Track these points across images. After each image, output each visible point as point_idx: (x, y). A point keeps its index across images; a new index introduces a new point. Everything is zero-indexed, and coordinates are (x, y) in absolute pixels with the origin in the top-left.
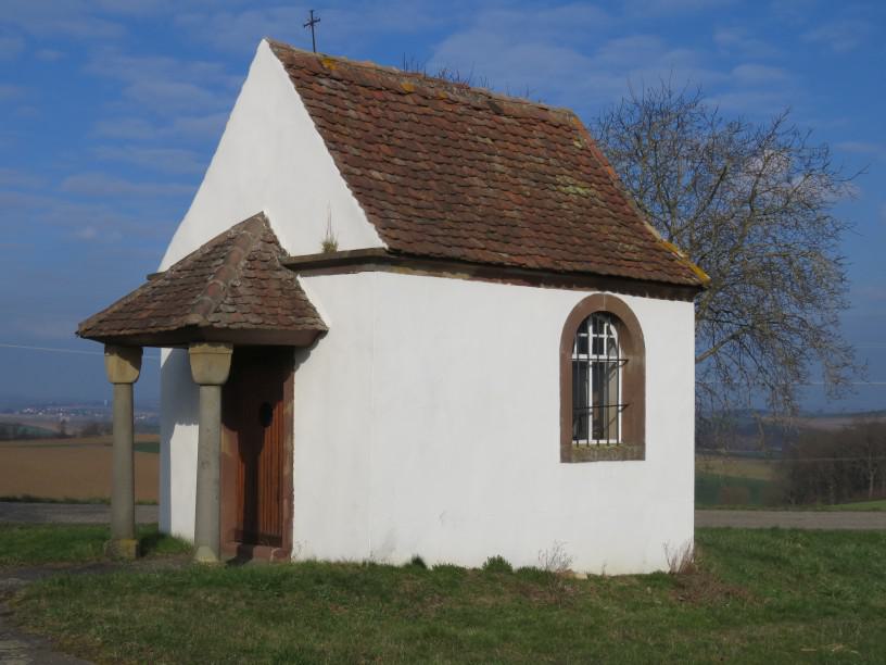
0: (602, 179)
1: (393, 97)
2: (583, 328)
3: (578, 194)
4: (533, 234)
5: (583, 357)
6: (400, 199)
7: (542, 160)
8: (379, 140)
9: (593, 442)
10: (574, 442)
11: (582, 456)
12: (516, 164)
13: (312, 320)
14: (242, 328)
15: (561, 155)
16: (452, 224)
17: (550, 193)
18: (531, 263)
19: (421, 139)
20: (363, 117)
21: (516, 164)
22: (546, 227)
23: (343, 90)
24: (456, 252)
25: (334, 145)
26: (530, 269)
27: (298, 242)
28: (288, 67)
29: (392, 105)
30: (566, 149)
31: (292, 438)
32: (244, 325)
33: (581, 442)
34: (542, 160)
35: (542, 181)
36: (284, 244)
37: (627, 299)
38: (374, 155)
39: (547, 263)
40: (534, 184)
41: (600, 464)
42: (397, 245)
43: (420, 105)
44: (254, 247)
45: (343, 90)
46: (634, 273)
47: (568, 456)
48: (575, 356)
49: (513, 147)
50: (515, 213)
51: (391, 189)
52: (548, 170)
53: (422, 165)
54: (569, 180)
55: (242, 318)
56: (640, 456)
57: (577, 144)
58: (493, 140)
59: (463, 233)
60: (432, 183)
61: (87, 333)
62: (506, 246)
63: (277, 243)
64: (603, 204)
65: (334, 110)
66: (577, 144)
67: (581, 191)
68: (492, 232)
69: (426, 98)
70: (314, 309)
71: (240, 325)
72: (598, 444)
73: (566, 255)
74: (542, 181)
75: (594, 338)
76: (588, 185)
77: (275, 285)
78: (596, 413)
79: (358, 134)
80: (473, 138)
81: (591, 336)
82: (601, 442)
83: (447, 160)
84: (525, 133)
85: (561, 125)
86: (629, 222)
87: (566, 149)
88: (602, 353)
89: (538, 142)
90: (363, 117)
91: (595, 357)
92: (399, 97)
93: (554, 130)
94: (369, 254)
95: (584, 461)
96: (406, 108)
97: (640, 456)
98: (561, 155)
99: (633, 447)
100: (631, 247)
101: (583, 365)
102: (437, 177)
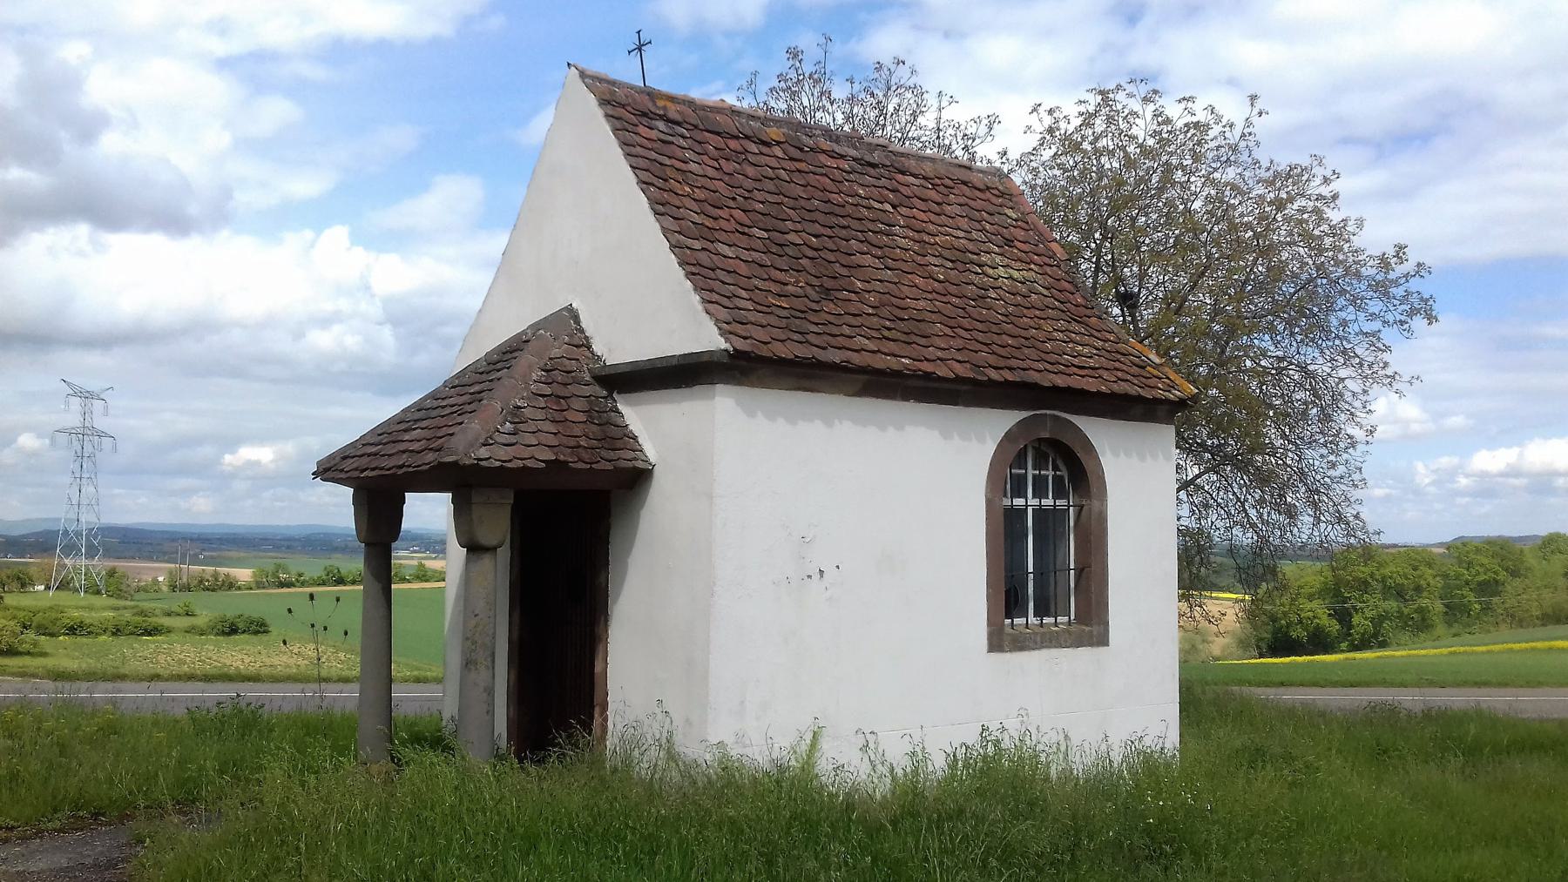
0: (1047, 260)
1: (753, 148)
2: (1020, 460)
3: (1011, 277)
4: (948, 331)
5: (1019, 502)
6: (756, 282)
7: (961, 234)
8: (731, 203)
9: (1032, 620)
10: (1008, 621)
11: (1021, 644)
12: (926, 238)
13: (631, 455)
14: (525, 468)
15: (988, 227)
16: (831, 318)
17: (972, 277)
18: (942, 371)
19: (792, 203)
20: (711, 172)
21: (926, 238)
22: (965, 323)
23: (684, 137)
24: (835, 356)
25: (660, 208)
26: (940, 379)
27: (619, 342)
28: (604, 102)
29: (751, 158)
30: (996, 219)
31: (606, 621)
32: (529, 463)
33: (1018, 621)
34: (961, 234)
35: (961, 259)
36: (598, 348)
37: (1082, 422)
38: (723, 224)
39: (963, 371)
40: (950, 265)
41: (1044, 652)
42: (742, 345)
43: (791, 159)
44: (555, 352)
45: (684, 137)
46: (1091, 385)
47: (998, 642)
48: (1007, 502)
49: (922, 216)
50: (922, 303)
51: (743, 269)
52: (971, 246)
53: (792, 237)
54: (998, 259)
55: (527, 453)
56: (1103, 640)
57: (1009, 212)
58: (894, 207)
59: (847, 330)
60: (803, 261)
61: (329, 470)
62: (908, 348)
63: (589, 347)
64: (1045, 292)
65: (667, 161)
66: (1009, 212)
67: (1016, 274)
68: (889, 329)
69: (801, 150)
70: (635, 438)
71: (520, 463)
72: (1042, 625)
73: (992, 360)
74: (961, 259)
75: (1034, 476)
76: (1024, 266)
77: (578, 404)
78: (1042, 578)
79: (699, 194)
80: (865, 202)
81: (1031, 472)
82: (1046, 620)
83: (828, 232)
84: (938, 198)
85: (988, 188)
86: (1083, 314)
87: (996, 219)
88: (1039, 513)
89: (957, 210)
90: (711, 172)
91: (1036, 502)
92: (765, 150)
93: (978, 194)
94: (705, 359)
95: (1022, 649)
96: (773, 163)
97: (1103, 640)
98: (988, 227)
99: (1091, 625)
100: (1086, 351)
101: (1023, 512)
102: (811, 253)
